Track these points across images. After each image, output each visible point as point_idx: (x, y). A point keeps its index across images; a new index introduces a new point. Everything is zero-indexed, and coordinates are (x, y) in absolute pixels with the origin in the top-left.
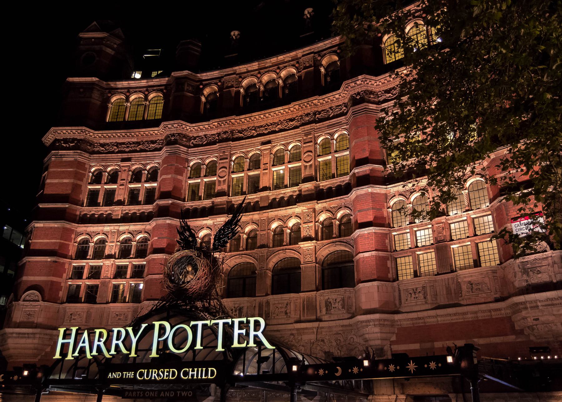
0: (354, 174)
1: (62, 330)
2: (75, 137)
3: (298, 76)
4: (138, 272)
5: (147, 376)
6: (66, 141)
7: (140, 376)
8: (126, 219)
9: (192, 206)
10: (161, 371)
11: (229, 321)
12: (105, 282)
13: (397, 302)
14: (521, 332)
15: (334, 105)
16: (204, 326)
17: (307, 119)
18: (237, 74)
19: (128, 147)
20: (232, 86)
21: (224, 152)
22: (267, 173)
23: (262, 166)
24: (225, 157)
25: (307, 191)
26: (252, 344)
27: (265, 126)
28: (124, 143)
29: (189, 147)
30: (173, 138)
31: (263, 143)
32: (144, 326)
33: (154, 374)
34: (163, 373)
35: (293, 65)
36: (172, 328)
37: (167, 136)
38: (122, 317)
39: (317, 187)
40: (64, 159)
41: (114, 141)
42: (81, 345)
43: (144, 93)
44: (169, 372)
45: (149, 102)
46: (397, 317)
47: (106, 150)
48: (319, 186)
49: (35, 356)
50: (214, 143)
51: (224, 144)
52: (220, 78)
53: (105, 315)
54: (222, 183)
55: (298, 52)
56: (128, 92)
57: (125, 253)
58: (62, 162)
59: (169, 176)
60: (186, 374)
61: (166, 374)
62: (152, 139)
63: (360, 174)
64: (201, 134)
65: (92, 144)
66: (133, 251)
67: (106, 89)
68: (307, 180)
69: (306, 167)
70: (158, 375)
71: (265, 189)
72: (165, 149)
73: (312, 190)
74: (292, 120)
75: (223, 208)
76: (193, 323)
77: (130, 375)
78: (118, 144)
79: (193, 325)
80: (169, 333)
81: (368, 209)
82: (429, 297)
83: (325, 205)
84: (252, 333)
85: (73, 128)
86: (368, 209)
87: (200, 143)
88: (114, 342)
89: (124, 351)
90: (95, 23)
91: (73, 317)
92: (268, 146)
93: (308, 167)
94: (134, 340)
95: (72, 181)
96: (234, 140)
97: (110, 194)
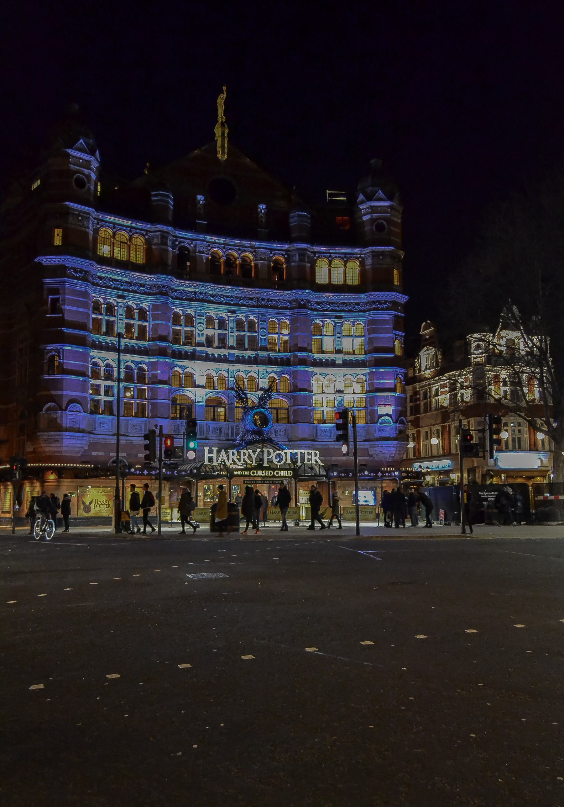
1: (207, 449)
9: (177, 349)
11: (303, 451)
13: (314, 435)
14: (371, 456)
18: (207, 242)
19: (122, 285)
21: (201, 310)
22: (233, 336)
26: (314, 462)
27: (230, 297)
28: (117, 280)
30: (164, 289)
31: (230, 311)
32: (258, 450)
35: (251, 252)
36: (274, 452)
40: (77, 288)
41: (109, 276)
42: (221, 458)
46: (315, 443)
50: (191, 300)
51: (201, 304)
54: (201, 336)
56: (114, 227)
57: (129, 378)
58: (75, 290)
59: (164, 323)
60: (277, 473)
61: (267, 473)
62: (142, 282)
63: (301, 357)
69: (261, 339)
71: (232, 348)
74: (251, 299)
75: (203, 356)
77: (247, 473)
80: (273, 455)
82: (332, 435)
83: (275, 370)
84: (314, 458)
87: (181, 297)
88: (242, 457)
89: (249, 462)
90: (82, 141)
92: (234, 315)
94: (254, 457)
95: (86, 311)
97: (110, 326)
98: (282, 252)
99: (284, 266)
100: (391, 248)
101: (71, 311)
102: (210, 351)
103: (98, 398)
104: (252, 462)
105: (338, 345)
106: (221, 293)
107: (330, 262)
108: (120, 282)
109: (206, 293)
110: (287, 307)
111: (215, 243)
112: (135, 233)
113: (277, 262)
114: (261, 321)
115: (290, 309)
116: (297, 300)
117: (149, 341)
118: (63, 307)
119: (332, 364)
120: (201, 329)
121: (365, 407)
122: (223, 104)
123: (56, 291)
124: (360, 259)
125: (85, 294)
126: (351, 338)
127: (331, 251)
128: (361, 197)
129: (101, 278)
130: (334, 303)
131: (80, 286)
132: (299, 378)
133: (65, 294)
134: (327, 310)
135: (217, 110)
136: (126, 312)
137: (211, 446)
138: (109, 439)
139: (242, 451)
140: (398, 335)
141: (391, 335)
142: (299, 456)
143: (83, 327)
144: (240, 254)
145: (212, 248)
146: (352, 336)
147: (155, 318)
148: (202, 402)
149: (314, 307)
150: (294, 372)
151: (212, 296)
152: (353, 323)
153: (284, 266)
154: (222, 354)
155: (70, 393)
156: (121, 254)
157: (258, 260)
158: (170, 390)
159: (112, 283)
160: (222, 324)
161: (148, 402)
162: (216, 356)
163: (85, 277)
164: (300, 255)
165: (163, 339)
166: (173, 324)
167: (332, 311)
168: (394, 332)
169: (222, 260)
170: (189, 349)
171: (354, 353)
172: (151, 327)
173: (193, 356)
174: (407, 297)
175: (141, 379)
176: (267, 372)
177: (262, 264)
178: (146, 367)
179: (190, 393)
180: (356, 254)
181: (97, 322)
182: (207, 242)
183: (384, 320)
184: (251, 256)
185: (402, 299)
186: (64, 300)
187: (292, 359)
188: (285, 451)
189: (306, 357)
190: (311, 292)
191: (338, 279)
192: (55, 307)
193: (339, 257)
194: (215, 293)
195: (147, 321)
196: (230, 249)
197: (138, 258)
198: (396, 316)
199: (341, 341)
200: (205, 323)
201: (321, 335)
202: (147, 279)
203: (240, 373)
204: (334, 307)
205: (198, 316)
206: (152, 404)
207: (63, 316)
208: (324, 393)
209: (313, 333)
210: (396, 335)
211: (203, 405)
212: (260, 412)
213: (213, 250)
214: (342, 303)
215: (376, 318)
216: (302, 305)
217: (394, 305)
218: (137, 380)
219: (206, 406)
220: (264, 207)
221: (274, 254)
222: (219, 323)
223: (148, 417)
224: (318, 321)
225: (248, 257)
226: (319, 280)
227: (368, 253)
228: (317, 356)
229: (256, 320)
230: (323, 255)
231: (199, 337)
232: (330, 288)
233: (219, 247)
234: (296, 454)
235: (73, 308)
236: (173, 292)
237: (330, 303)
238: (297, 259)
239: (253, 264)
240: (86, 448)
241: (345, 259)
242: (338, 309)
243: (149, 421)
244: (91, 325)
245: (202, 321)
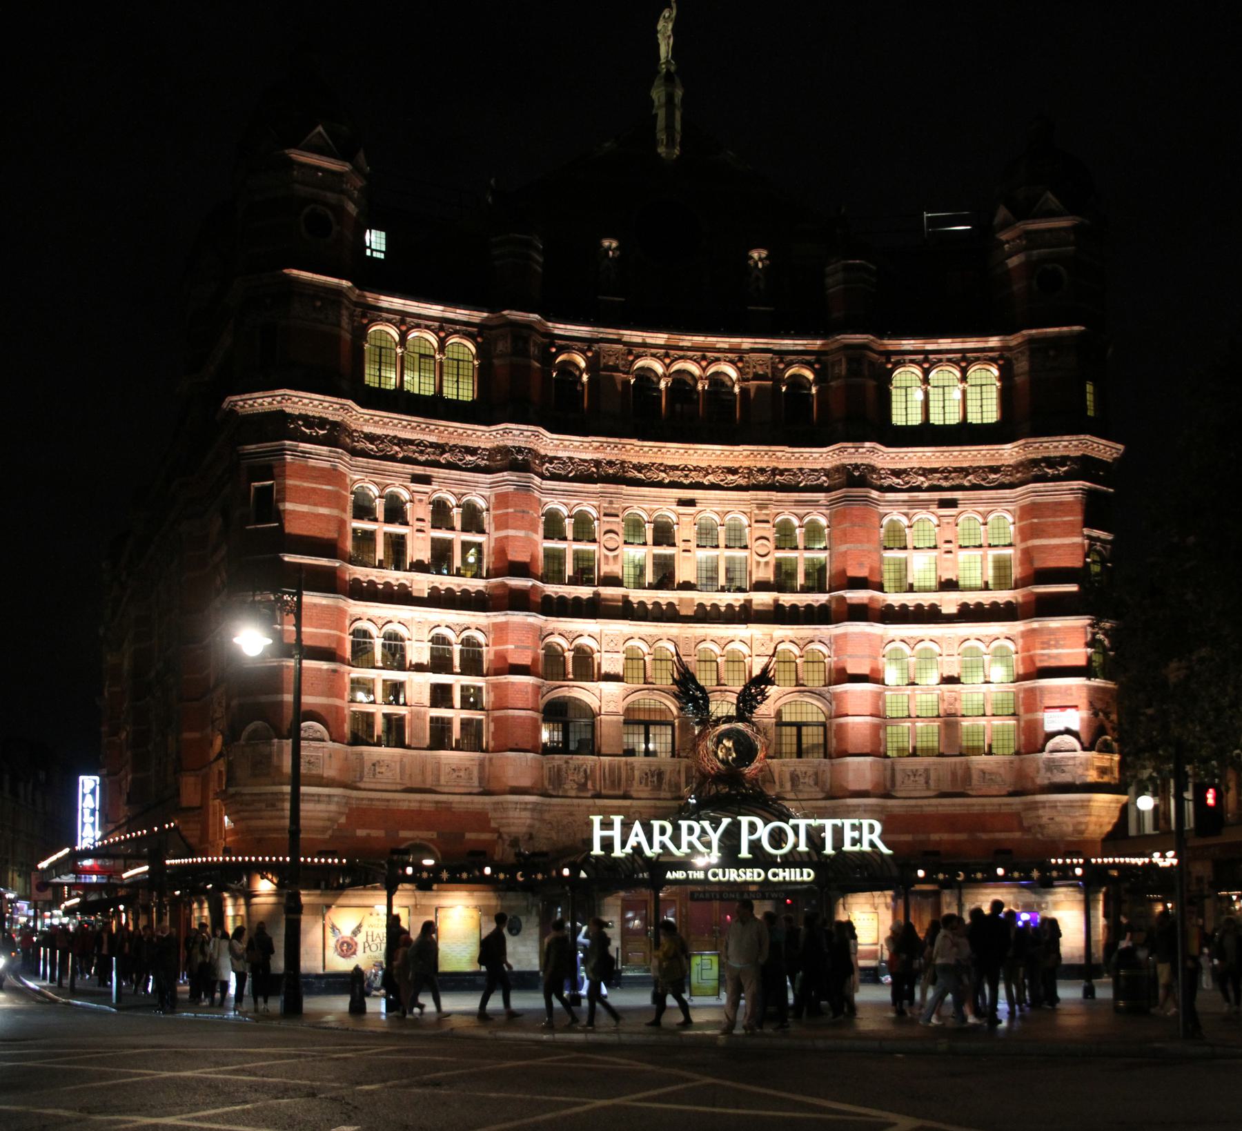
0: (844, 599)
3: (741, 388)
4: (471, 700)
6: (308, 420)
9: (556, 593)
12: (419, 712)
15: (807, 466)
16: (809, 827)
17: (762, 479)
20: (615, 369)
21: (611, 502)
22: (689, 558)
24: (613, 511)
27: (683, 470)
31: (682, 503)
35: (732, 362)
38: (462, 774)
49: (324, 830)
51: (611, 488)
52: (590, 341)
53: (429, 768)
54: (611, 560)
55: (745, 340)
57: (440, 663)
59: (521, 533)
62: (469, 444)
63: (854, 601)
64: (563, 454)
66: (457, 661)
68: (761, 586)
69: (758, 563)
71: (687, 586)
73: (768, 605)
81: (862, 657)
86: (862, 657)
87: (563, 473)
91: (378, 770)
93: (762, 565)
98: (808, 358)
99: (814, 390)
100: (1076, 328)
101: (302, 512)
102: (636, 596)
105: (947, 569)
106: (659, 461)
107: (926, 373)
108: (418, 445)
109: (623, 462)
110: (821, 485)
111: (644, 345)
112: (451, 334)
113: (797, 380)
114: (757, 521)
115: (827, 490)
116: (844, 466)
117: (487, 578)
118: (281, 507)
119: (931, 615)
120: (611, 545)
121: (1014, 714)
122: (669, 33)
123: (267, 472)
124: (1001, 362)
125: (334, 476)
126: (979, 552)
127: (929, 347)
128: (1002, 213)
130: (935, 470)
131: (321, 455)
132: (850, 650)
133: (283, 476)
134: (918, 489)
135: (658, 46)
136: (433, 512)
137: (606, 812)
138: (394, 800)
139: (684, 824)
140: (1098, 539)
141: (1078, 540)
142: (828, 836)
143: (328, 548)
144: (704, 369)
145: (638, 357)
146: (981, 546)
147: (501, 523)
148: (616, 714)
149: (886, 482)
150: (837, 637)
151: (639, 468)
152: (985, 515)
153: (814, 390)
154: (663, 602)
156: (419, 383)
157: (748, 380)
158: (538, 688)
159: (397, 448)
160: (664, 534)
161: (488, 716)
162: (650, 607)
163: (334, 435)
164: (850, 361)
165: (521, 569)
166: (545, 538)
167: (932, 489)
168: (1086, 531)
169: (662, 385)
170: (585, 592)
171: (986, 587)
172: (492, 544)
173: (593, 609)
174: (1121, 447)
175: (472, 664)
176: (771, 640)
177: (759, 388)
178: (481, 638)
179: (590, 694)
180: (992, 349)
181: (366, 539)
182: (625, 344)
183: (1061, 503)
184: (732, 372)
185: (1105, 449)
186: (282, 490)
187: (833, 606)
188: (792, 822)
189: (866, 601)
190: (878, 446)
191: (946, 414)
192: (268, 505)
193: (949, 360)
194: (645, 461)
195: (482, 532)
196: (681, 358)
197: (463, 390)
198: (1089, 493)
199: (955, 562)
200: (621, 532)
201: (905, 548)
202: (484, 437)
203: (708, 645)
204: (936, 480)
205: (606, 515)
206: (497, 720)
207: (282, 526)
208: (913, 684)
209: (886, 544)
210: (1089, 537)
211: (618, 721)
212: (739, 732)
213: (640, 363)
214: (956, 470)
215: (1039, 499)
216: (856, 479)
217: (1084, 467)
218: (461, 666)
219: (626, 722)
220: (764, 253)
221: (789, 365)
222: (655, 530)
223: (486, 751)
224: (895, 515)
225: (726, 375)
226: (898, 419)
227: (1020, 345)
228: (895, 599)
229: (745, 521)
230: (908, 357)
231: (607, 564)
232: (927, 434)
233: (653, 355)
234: (822, 829)
235: (304, 508)
236: (543, 464)
237: (926, 472)
238: (843, 373)
239: (737, 389)
240: (343, 820)
241: (963, 364)
242: (945, 484)
243: (491, 760)
244: (349, 545)
245: (614, 527)
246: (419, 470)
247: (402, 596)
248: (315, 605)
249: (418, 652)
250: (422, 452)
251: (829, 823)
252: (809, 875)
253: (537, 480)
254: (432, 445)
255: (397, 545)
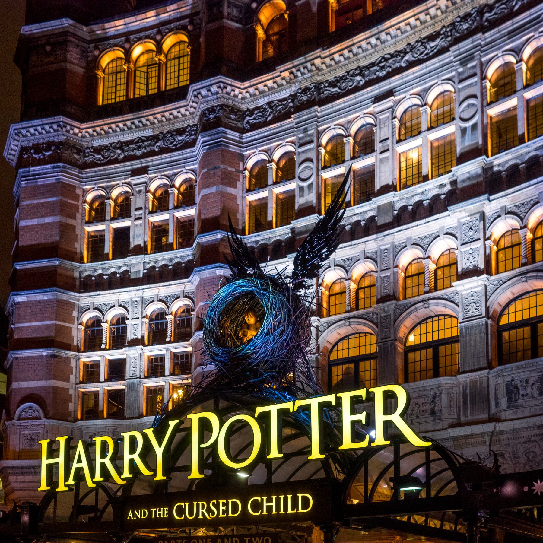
2: (51, 139)
5: (191, 514)
6: (37, 148)
7: (179, 515)
8: (153, 277)
10: (213, 504)
16: (282, 413)
22: (387, 158)
23: (378, 146)
25: (469, 179)
29: (242, 131)
33: (201, 511)
34: (217, 506)
37: (203, 114)
39: (487, 169)
43: (154, 39)
44: (226, 505)
45: (166, 56)
47: (106, 156)
48: (492, 167)
61: (221, 508)
65: (81, 151)
67: (90, 42)
70: (209, 511)
72: (200, 140)
73: (478, 176)
76: (260, 410)
78: (122, 145)
79: (261, 414)
85: (45, 121)
96: (322, 102)
103: (94, 387)
104: (151, 466)
129: (98, 150)
155: (24, 384)
246: (136, 164)
247: (123, 281)
248: (39, 302)
249: (136, 328)
250: (139, 148)
251: (314, 403)
252: (306, 502)
253: (233, 135)
254: (148, 138)
255: (122, 236)
